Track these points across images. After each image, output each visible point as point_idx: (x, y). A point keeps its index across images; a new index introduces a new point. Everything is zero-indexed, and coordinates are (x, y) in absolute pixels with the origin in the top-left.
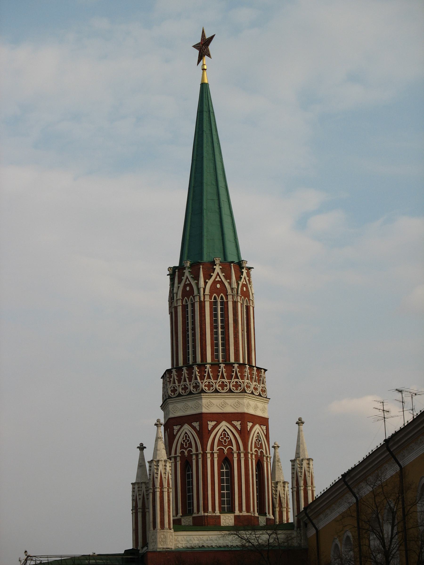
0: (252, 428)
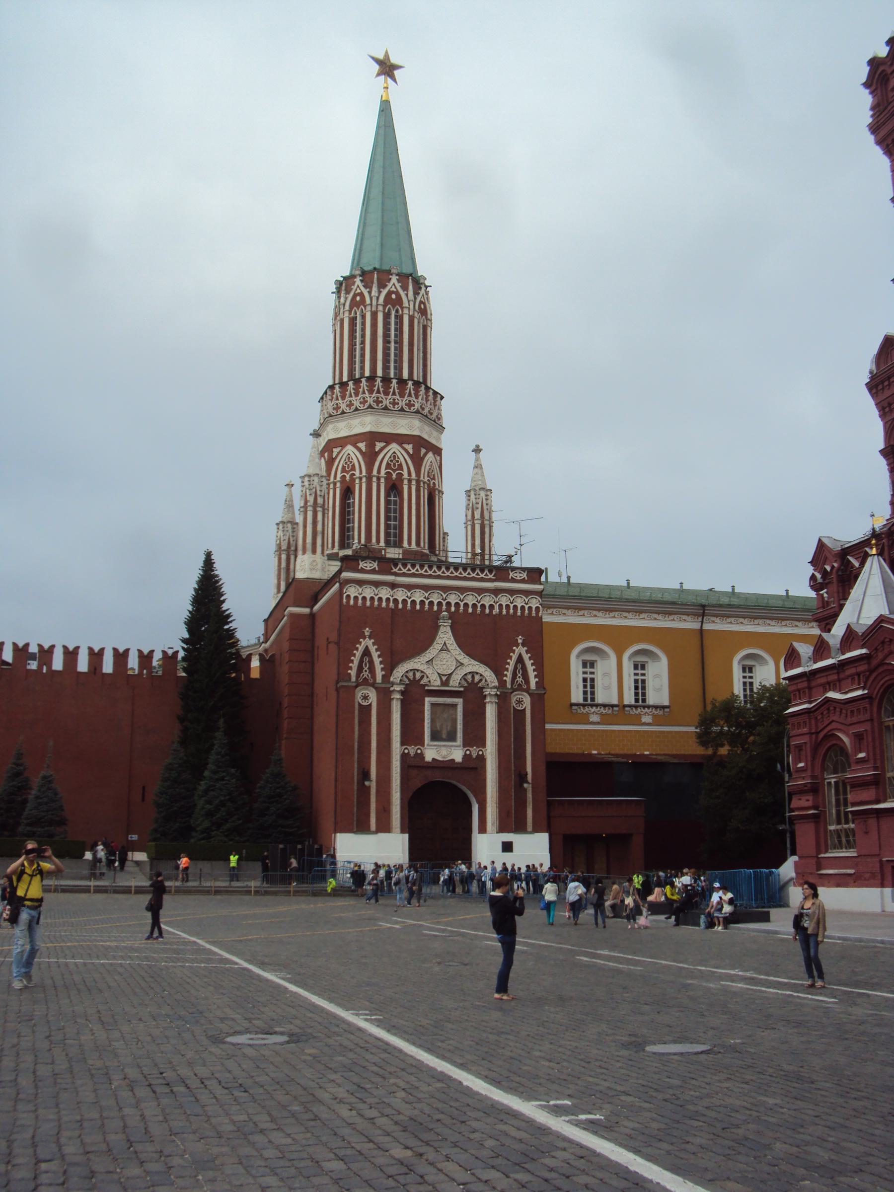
0: (426, 454)
